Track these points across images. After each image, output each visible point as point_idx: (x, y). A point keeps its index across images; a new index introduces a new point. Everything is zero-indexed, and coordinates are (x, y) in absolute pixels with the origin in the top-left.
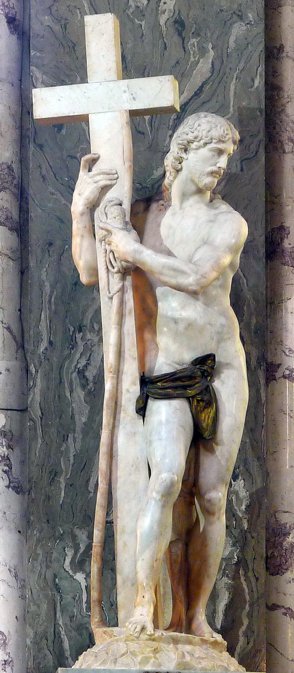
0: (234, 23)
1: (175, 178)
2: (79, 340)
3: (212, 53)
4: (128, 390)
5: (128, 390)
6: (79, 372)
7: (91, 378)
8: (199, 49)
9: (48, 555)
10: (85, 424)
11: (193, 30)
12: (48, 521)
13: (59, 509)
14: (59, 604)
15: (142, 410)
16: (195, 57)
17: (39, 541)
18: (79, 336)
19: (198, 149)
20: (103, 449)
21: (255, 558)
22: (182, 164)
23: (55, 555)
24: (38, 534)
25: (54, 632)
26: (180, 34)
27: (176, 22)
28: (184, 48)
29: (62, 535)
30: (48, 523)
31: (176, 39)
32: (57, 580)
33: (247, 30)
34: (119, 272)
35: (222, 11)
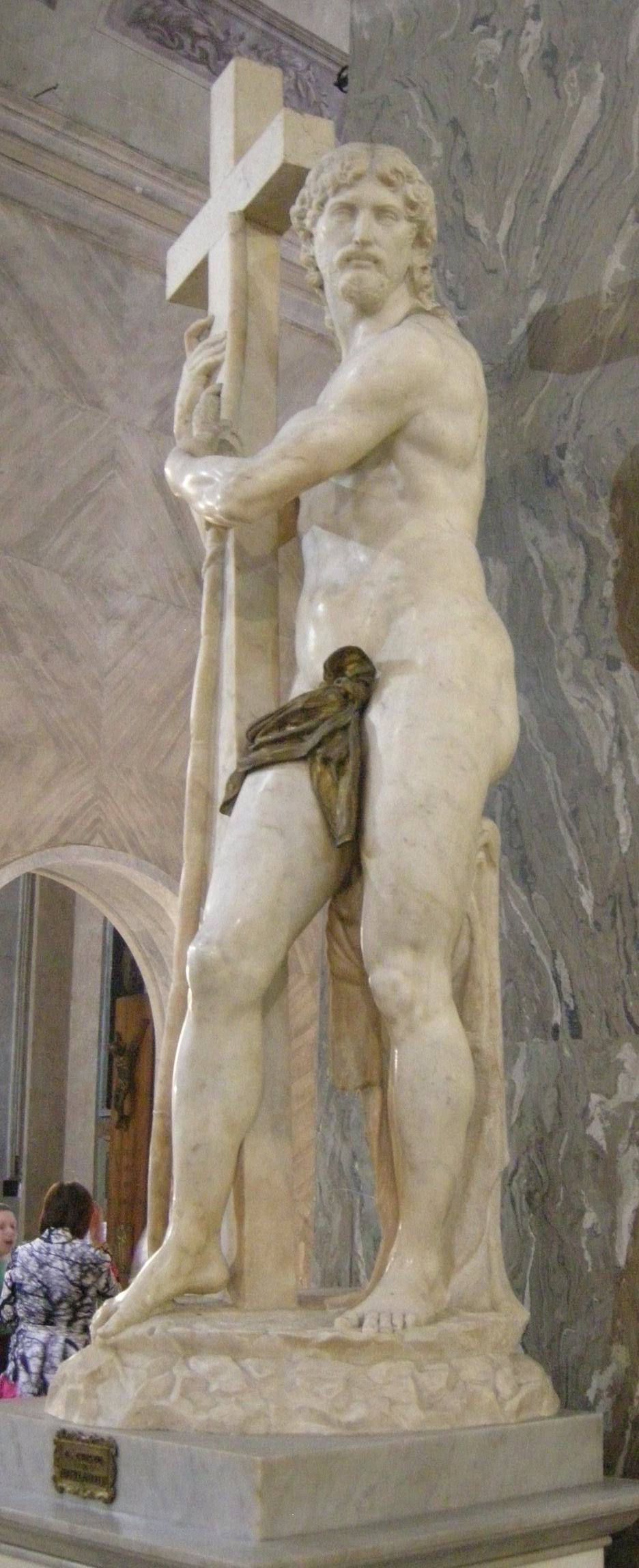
3: (601, 77)
5: (225, 770)
11: (572, 53)
14: (358, 1214)
16: (574, 99)
23: (354, 1115)
25: (351, 1270)
27: (546, 55)
28: (557, 92)
32: (357, 1166)
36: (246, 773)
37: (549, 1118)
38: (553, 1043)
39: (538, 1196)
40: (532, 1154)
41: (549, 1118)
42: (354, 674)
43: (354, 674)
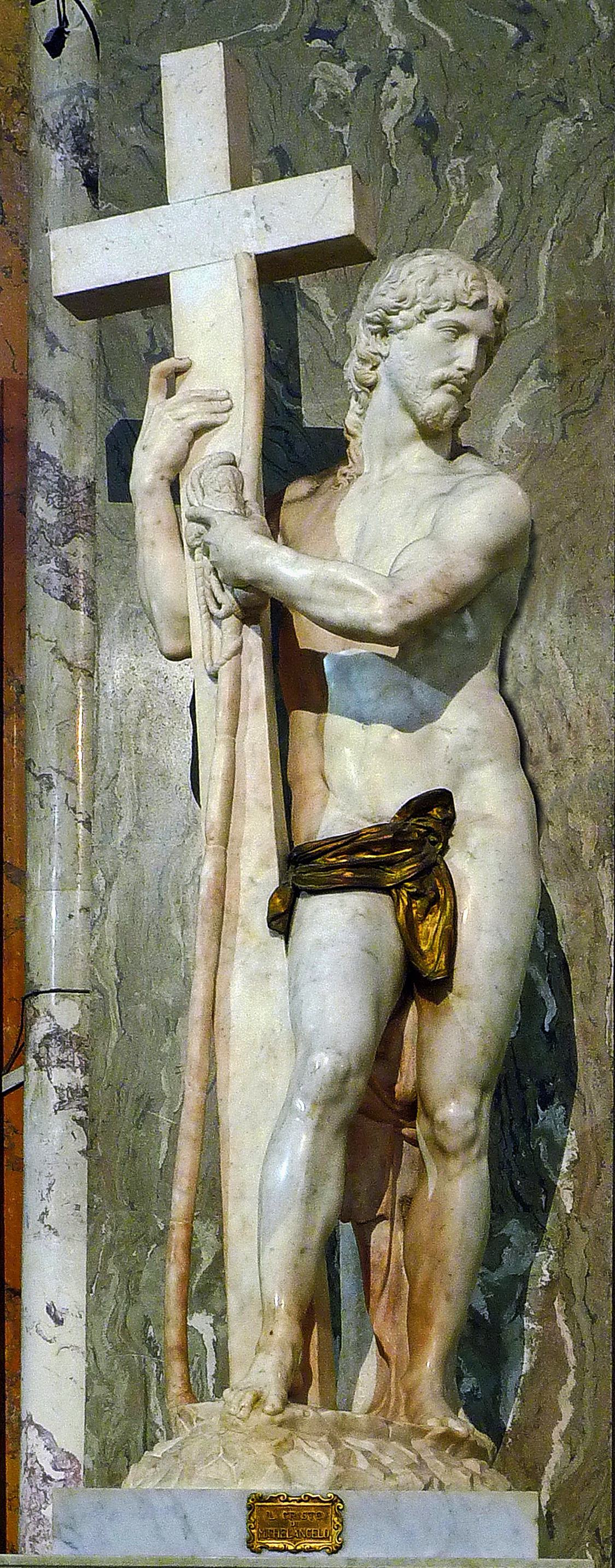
0: (549, 119)
4: (252, 880)
8: (469, 179)
9: (131, 1278)
12: (131, 1204)
13: (157, 1178)
15: (282, 922)
16: (460, 198)
17: (111, 1246)
20: (197, 1010)
21: (588, 1275)
24: (110, 1233)
26: (427, 150)
27: (417, 124)
28: (436, 179)
29: (162, 1233)
30: (132, 1209)
31: (420, 158)
33: (577, 133)
35: (520, 94)
36: (296, 893)
42: (431, 817)
43: (431, 817)
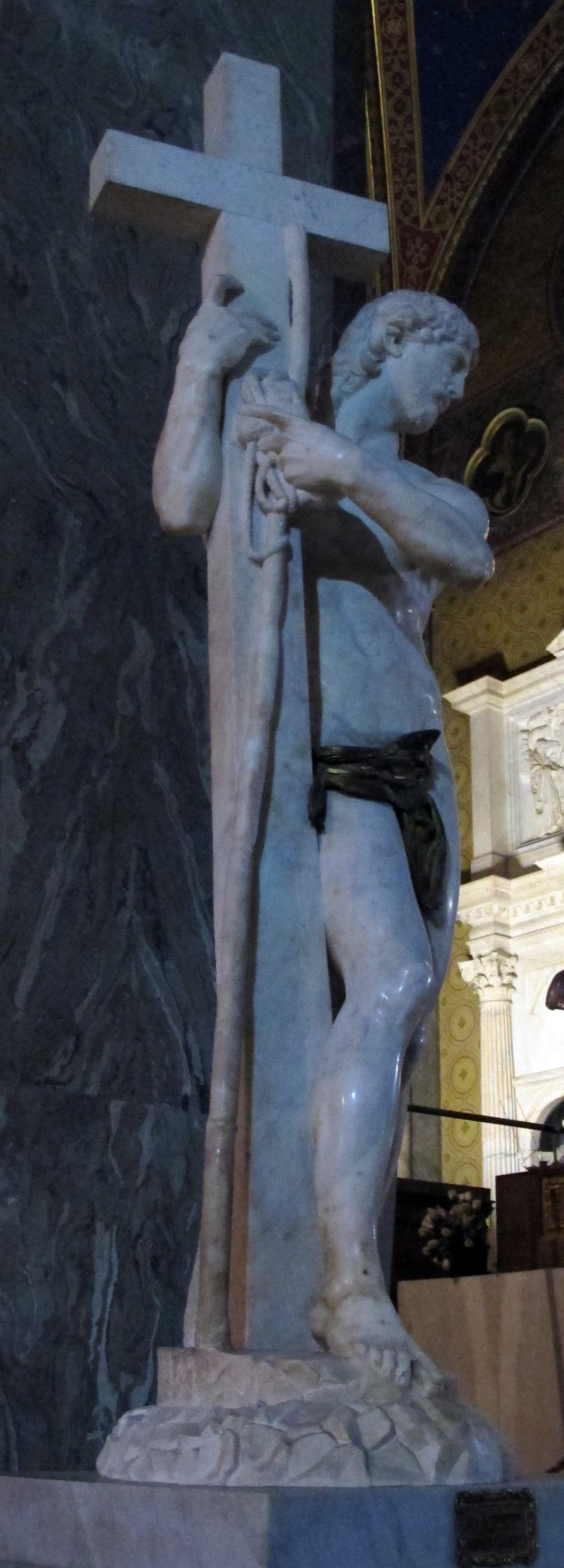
1: (357, 388)
2: (20, 686)
5: (286, 766)
6: (15, 748)
7: (36, 767)
10: (18, 858)
18: (21, 676)
19: (429, 341)
22: (382, 366)
34: (285, 511)
37: (177, 1184)
38: (182, 1113)
39: (163, 1263)
40: (159, 1219)
41: (177, 1184)
